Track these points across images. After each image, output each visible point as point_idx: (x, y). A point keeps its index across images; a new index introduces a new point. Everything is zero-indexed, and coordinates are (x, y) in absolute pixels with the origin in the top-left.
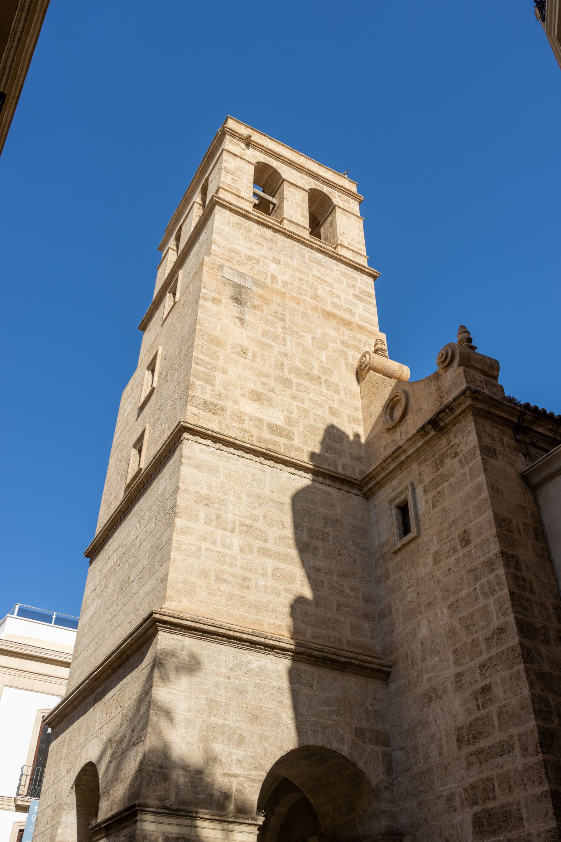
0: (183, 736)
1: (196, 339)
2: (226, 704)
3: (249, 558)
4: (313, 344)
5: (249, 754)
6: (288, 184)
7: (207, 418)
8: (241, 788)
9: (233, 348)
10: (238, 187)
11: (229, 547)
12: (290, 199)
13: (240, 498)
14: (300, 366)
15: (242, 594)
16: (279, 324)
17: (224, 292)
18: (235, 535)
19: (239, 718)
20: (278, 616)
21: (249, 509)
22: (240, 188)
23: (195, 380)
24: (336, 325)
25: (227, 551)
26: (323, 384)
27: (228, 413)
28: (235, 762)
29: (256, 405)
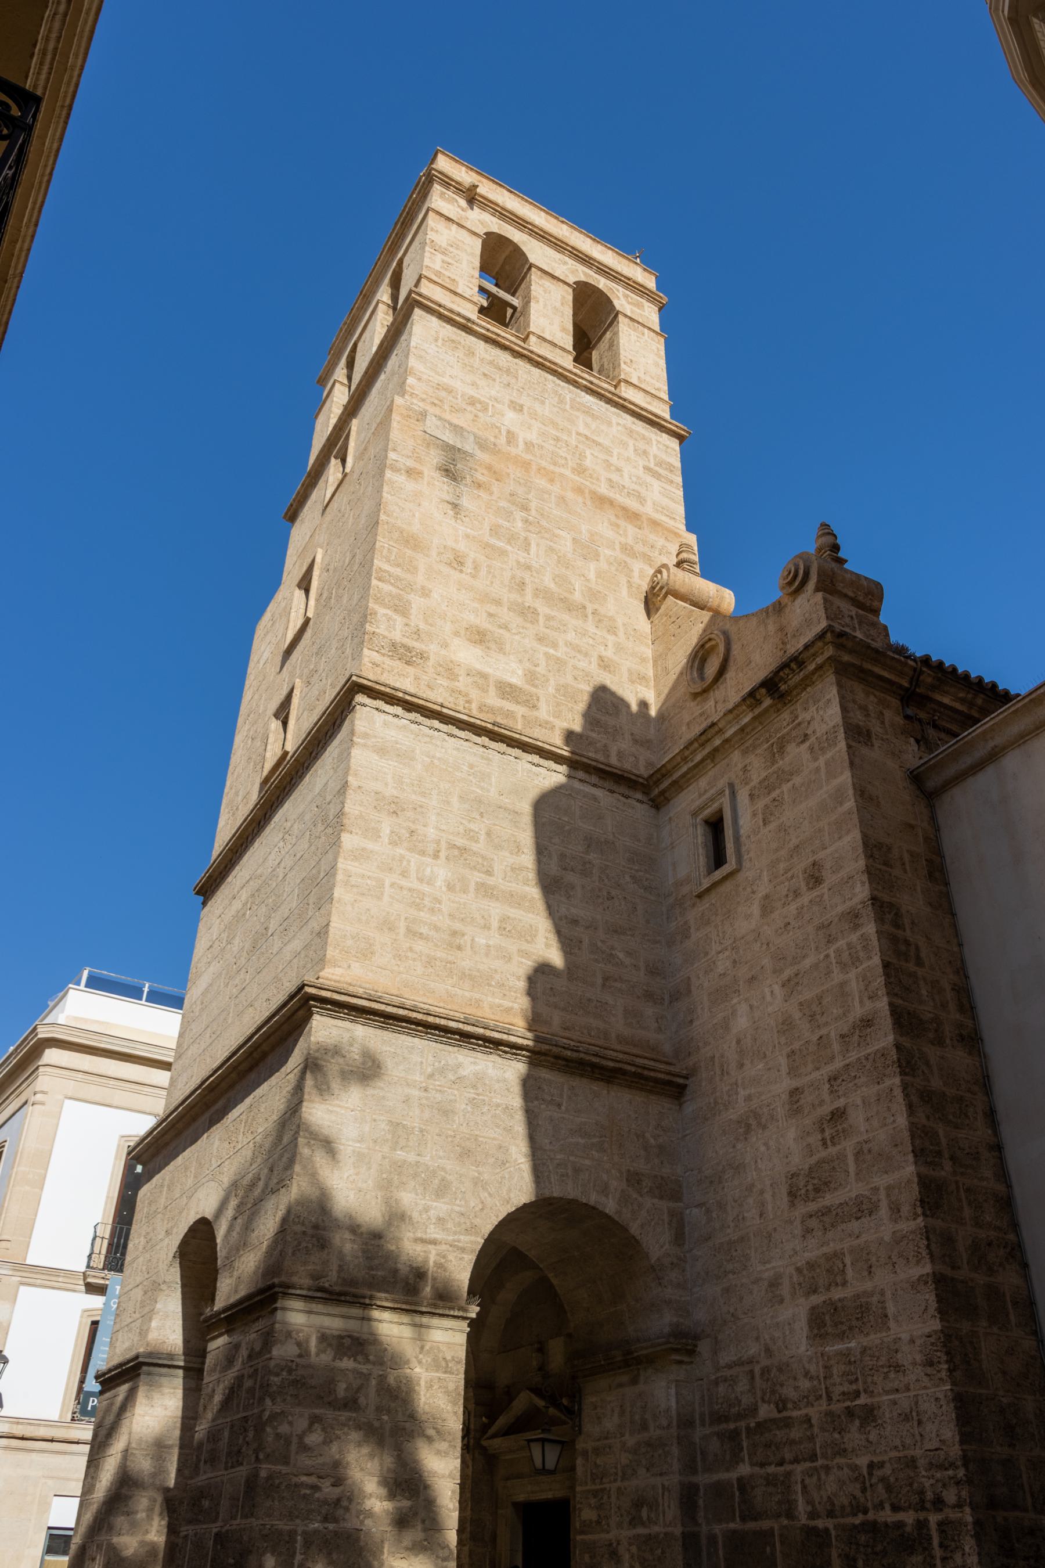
0: (351, 1179)
1: (379, 538)
2: (421, 1131)
3: (462, 901)
4: (574, 550)
5: (457, 1209)
6: (539, 273)
7: (396, 671)
8: (443, 1261)
9: (440, 554)
10: (453, 277)
11: (430, 882)
12: (541, 300)
13: (448, 803)
14: (552, 586)
15: (450, 958)
16: (519, 515)
17: (427, 459)
18: (439, 862)
19: (441, 1154)
20: (507, 993)
21: (464, 822)
22: (457, 278)
23: (376, 607)
24: (613, 518)
25: (426, 889)
26: (590, 617)
27: (430, 663)
28: (434, 1221)
29: (478, 651)
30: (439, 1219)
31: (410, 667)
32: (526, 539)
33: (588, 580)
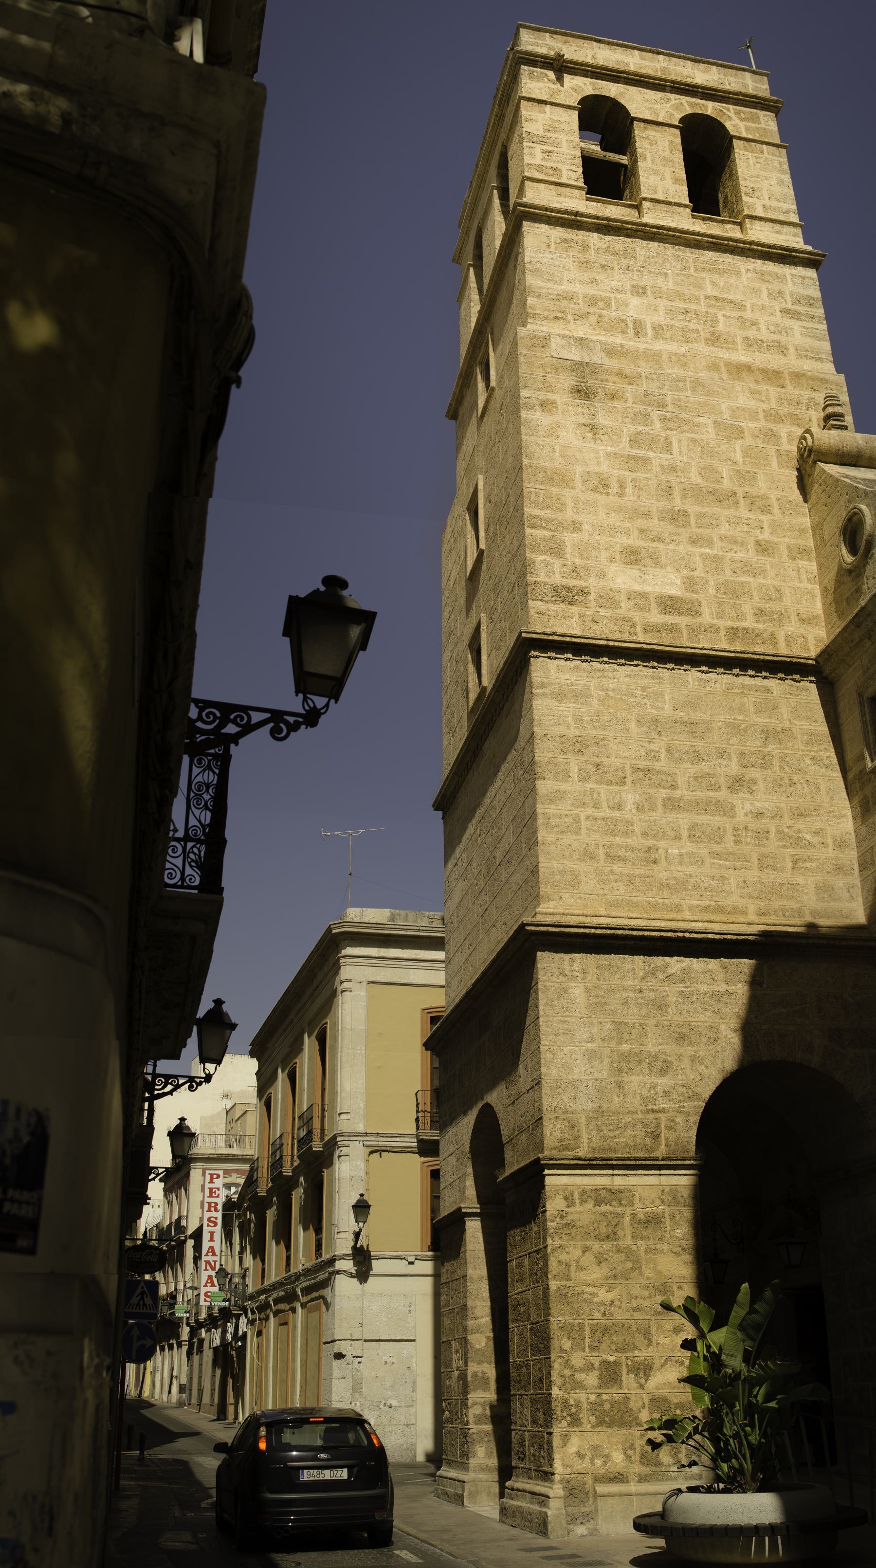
0: (588, 1072)
1: (525, 484)
2: (641, 1025)
3: (652, 819)
4: (717, 434)
5: (680, 1082)
6: (642, 124)
7: (561, 614)
8: (672, 1124)
9: (585, 481)
10: (554, 165)
11: (619, 807)
12: (649, 155)
13: (627, 730)
14: (699, 481)
15: (648, 873)
16: (656, 414)
17: (558, 385)
18: (626, 788)
19: (660, 1041)
20: (704, 894)
21: (644, 744)
22: (559, 166)
23: (533, 555)
24: (753, 386)
25: (617, 814)
26: (742, 502)
27: (592, 597)
28: (661, 1094)
29: (635, 572)
30: (665, 1092)
31: (573, 607)
32: (666, 438)
33: (735, 463)
